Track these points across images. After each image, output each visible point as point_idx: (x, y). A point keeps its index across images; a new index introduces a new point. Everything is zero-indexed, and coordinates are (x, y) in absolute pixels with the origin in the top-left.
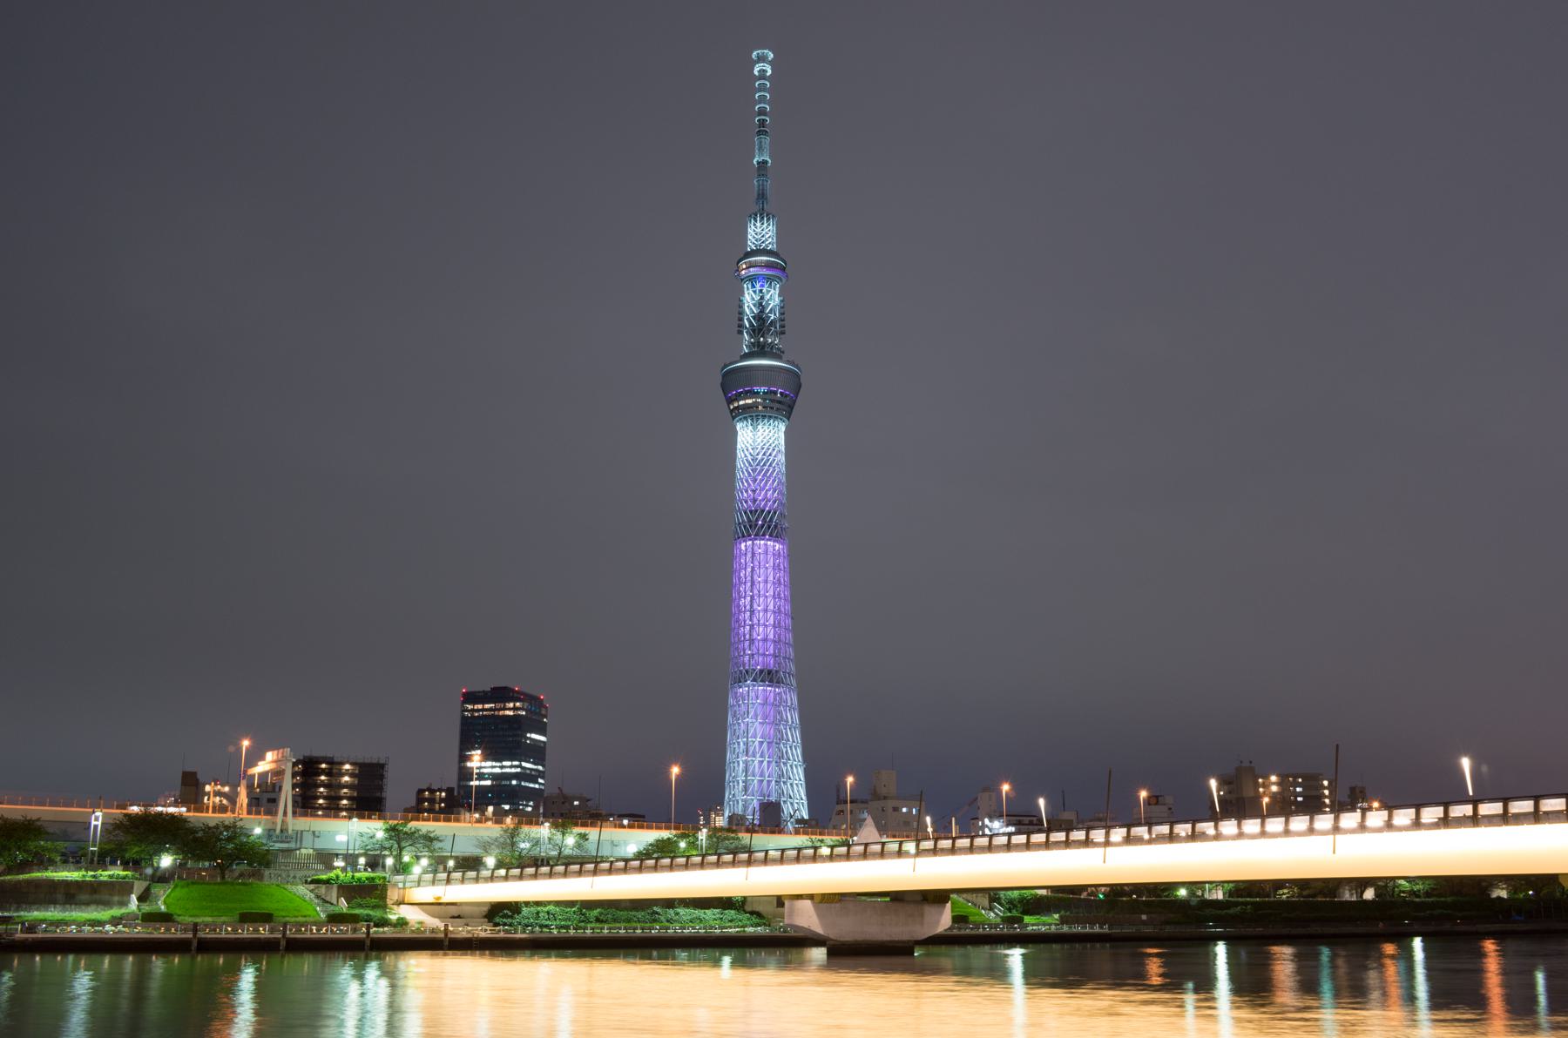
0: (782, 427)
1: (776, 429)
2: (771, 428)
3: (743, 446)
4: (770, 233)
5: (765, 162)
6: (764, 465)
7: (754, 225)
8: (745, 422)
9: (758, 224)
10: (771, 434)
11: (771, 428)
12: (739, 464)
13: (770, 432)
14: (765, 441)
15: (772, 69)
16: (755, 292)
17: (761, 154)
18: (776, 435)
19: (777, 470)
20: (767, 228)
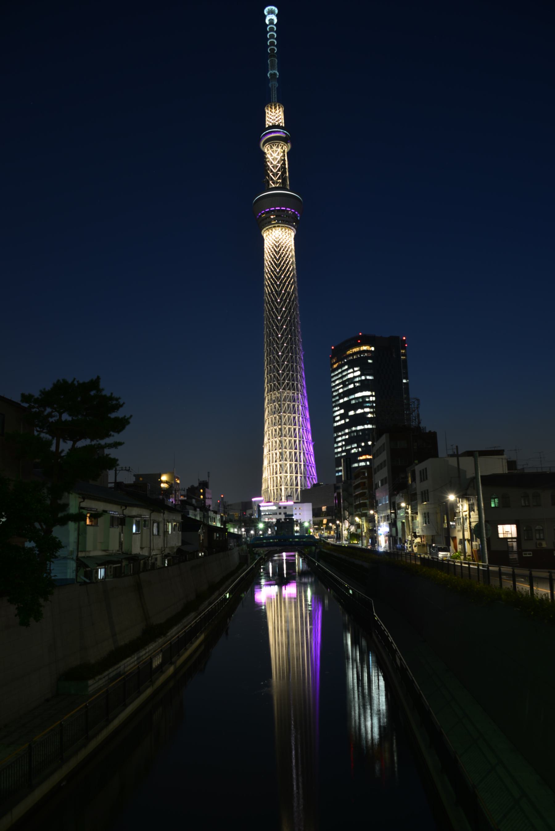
0: (293, 234)
1: (290, 235)
2: (287, 234)
3: (270, 246)
4: (281, 117)
5: (275, 74)
6: (284, 256)
7: (271, 111)
8: (270, 231)
9: (273, 110)
10: (287, 238)
11: (287, 234)
12: (267, 256)
13: (286, 236)
14: (284, 242)
15: (277, 19)
16: (273, 151)
17: (273, 68)
18: (290, 240)
19: (291, 260)
20: (279, 113)
